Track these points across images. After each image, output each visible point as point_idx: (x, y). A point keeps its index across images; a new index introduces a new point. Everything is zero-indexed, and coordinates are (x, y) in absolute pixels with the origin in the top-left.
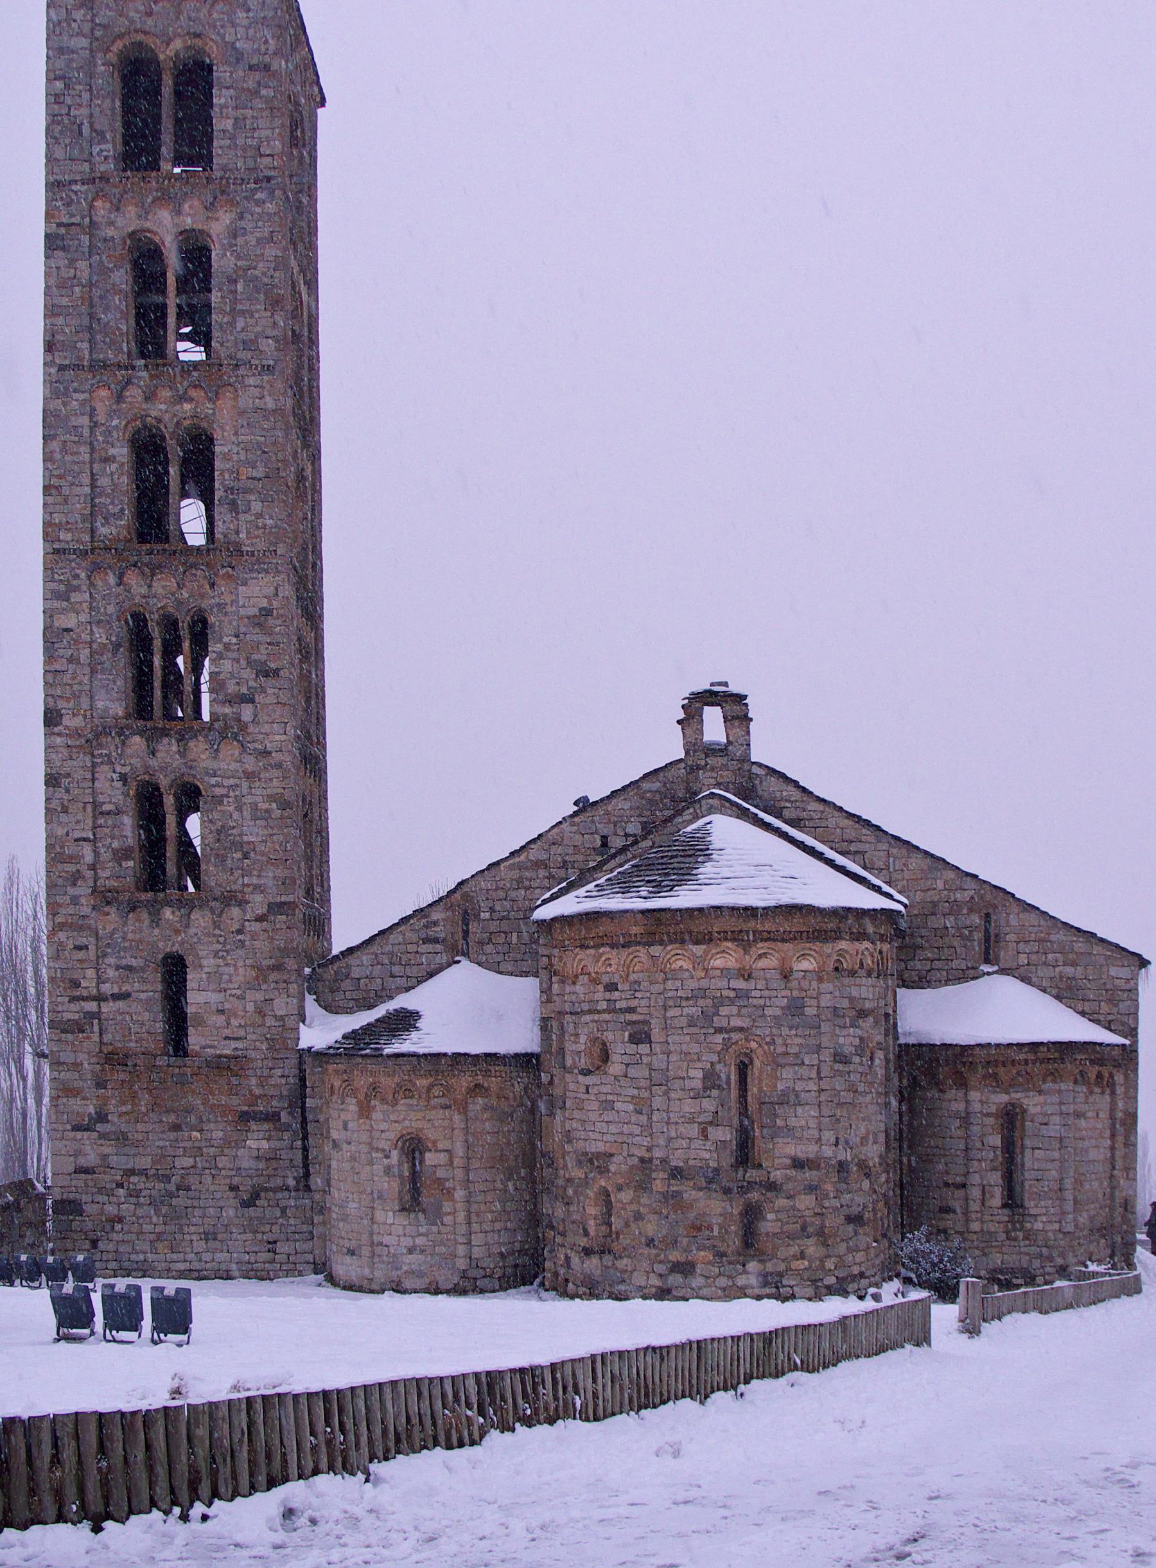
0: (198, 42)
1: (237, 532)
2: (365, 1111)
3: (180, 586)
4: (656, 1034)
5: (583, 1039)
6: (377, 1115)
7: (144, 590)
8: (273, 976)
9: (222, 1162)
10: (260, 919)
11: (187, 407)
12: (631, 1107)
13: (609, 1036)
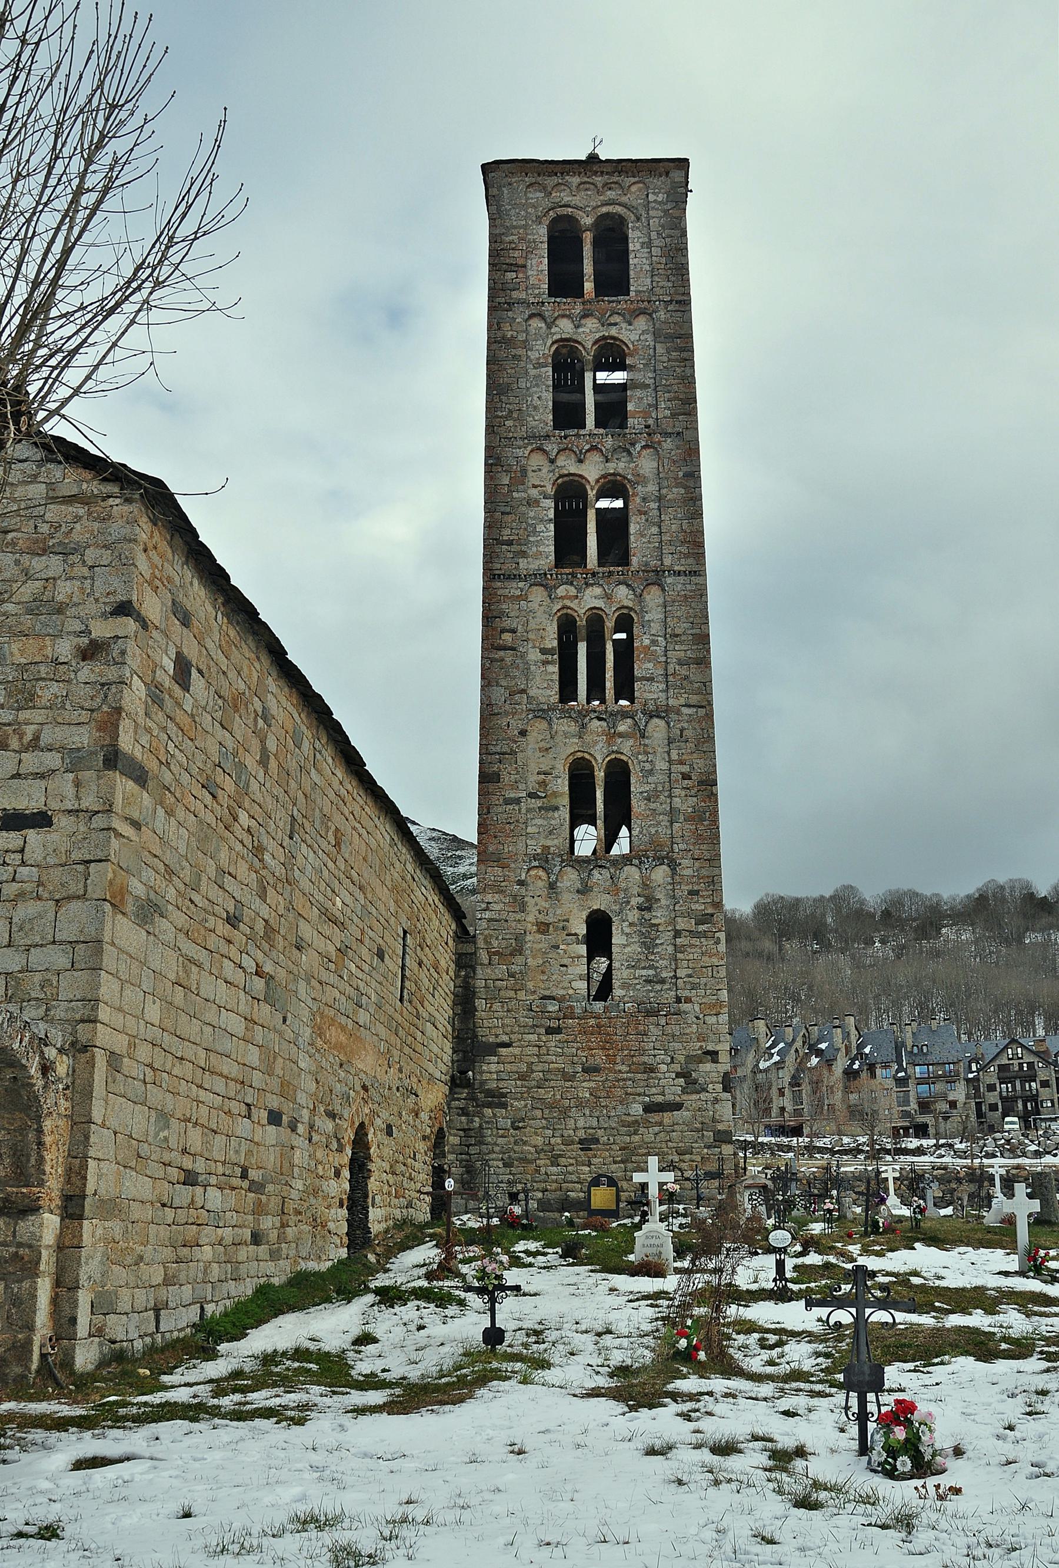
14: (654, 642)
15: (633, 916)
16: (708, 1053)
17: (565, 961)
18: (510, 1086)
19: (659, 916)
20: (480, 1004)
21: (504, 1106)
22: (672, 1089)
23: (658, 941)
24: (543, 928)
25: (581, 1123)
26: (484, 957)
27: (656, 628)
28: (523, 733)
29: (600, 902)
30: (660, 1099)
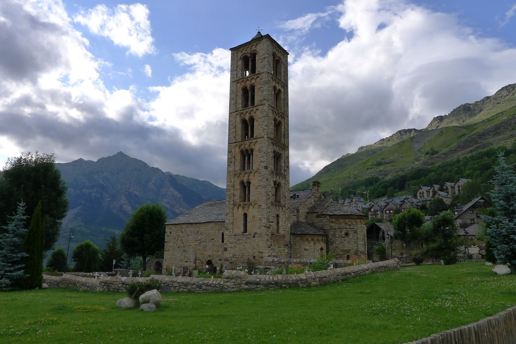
0: (280, 59)
1: (284, 142)
2: (315, 244)
3: (279, 149)
4: (358, 232)
5: (343, 233)
6: (317, 244)
7: (276, 148)
8: (288, 220)
9: (283, 254)
10: (287, 210)
11: (280, 118)
12: (354, 243)
13: (350, 232)
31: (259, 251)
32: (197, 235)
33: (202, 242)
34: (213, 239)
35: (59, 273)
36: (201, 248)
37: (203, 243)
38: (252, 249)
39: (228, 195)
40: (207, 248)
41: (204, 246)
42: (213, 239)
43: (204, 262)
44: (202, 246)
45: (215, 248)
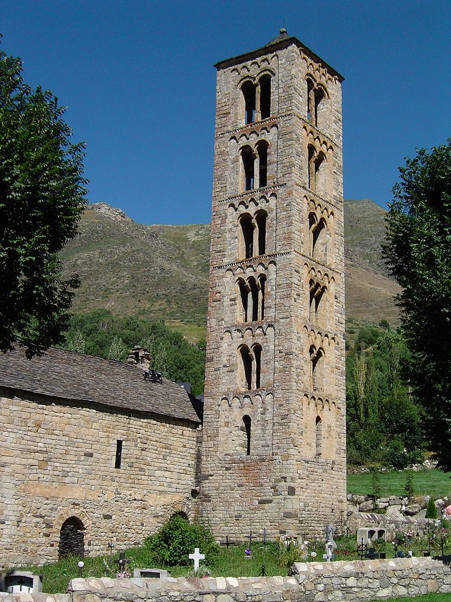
14: (272, 289)
15: (259, 417)
16: (283, 478)
17: (234, 438)
18: (213, 493)
19: (268, 416)
20: (204, 458)
21: (210, 501)
22: (268, 493)
23: (267, 428)
24: (227, 424)
25: (235, 508)
26: (205, 437)
27: (273, 282)
28: (222, 339)
29: (247, 411)
30: (264, 498)
31: (338, 497)
32: (33, 434)
33: (50, 460)
34: (91, 455)
35: (248, 557)
36: (49, 477)
37: (58, 464)
38: (330, 494)
39: (294, 366)
40: (67, 480)
41: (56, 473)
42: (91, 455)
43: (55, 523)
44: (51, 472)
45: (94, 482)
